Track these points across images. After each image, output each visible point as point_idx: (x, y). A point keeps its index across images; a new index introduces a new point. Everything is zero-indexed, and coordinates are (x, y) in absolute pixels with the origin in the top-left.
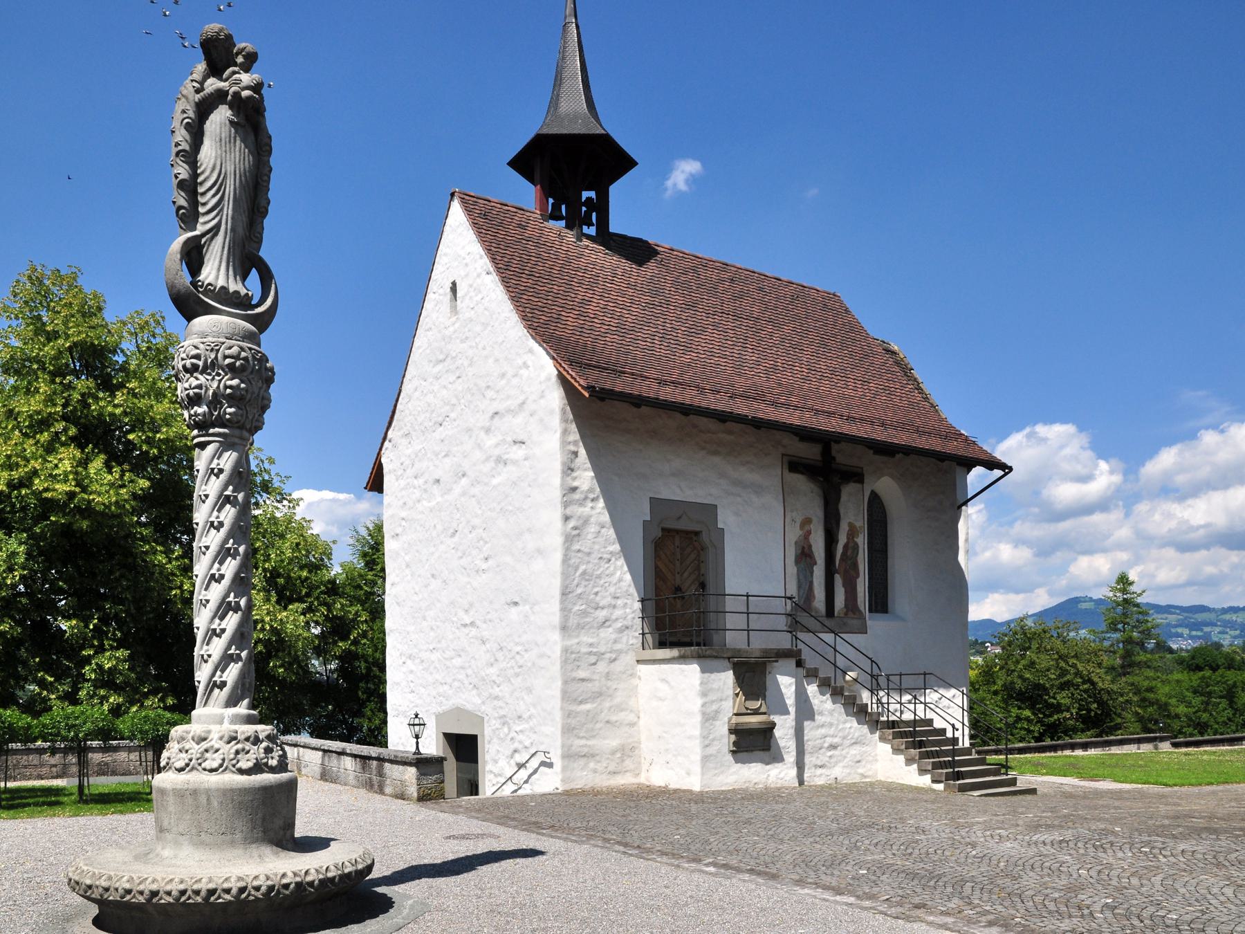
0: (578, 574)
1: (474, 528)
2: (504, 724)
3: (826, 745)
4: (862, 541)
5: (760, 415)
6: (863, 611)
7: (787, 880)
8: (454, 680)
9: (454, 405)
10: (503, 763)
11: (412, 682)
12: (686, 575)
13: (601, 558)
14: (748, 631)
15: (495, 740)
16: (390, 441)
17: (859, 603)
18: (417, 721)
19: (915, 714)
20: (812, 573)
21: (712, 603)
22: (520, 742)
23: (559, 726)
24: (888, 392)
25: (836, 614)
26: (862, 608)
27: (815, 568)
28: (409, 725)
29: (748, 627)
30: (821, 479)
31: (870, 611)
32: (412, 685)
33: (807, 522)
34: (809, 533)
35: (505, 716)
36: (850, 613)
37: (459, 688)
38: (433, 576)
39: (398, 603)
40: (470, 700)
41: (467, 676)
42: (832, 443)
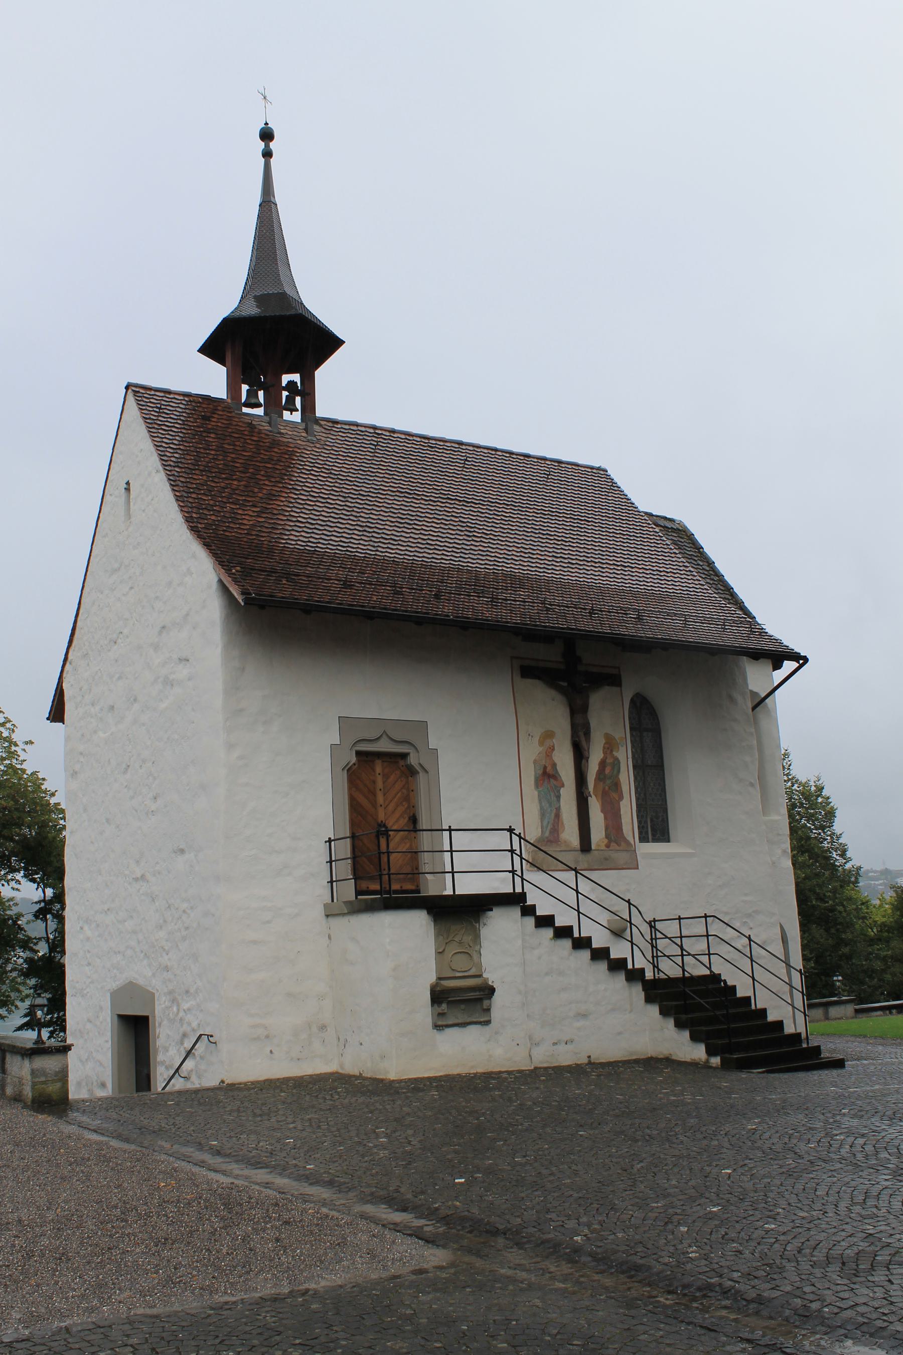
1: (144, 761)
4: (625, 756)
9: (127, 620)
10: (172, 1051)
11: (89, 952)
12: (391, 807)
15: (165, 1022)
16: (70, 663)
17: (624, 831)
19: (684, 970)
20: (558, 797)
25: (593, 847)
26: (630, 839)
27: (562, 791)
29: (453, 868)
30: (565, 684)
32: (88, 955)
33: (548, 735)
36: (612, 844)
38: (108, 820)
41: (139, 942)
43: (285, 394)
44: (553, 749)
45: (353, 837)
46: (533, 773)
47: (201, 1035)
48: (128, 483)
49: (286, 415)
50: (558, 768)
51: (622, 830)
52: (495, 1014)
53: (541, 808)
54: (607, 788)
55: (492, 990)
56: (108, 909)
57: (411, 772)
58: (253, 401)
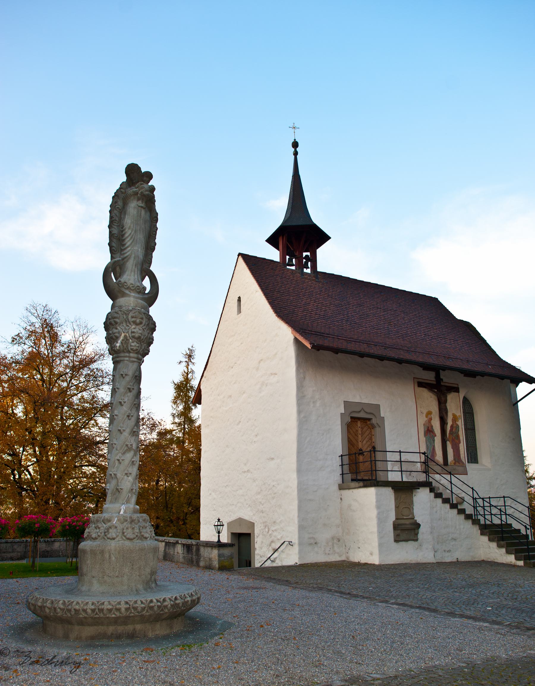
0: (306, 441)
2: (266, 527)
3: (450, 538)
4: (461, 423)
5: (401, 357)
6: (465, 462)
7: (443, 613)
8: (238, 502)
10: (265, 549)
12: (364, 442)
13: (318, 433)
14: (401, 471)
17: (461, 457)
18: (219, 524)
19: (501, 520)
20: (434, 441)
21: (379, 456)
22: (275, 536)
23: (297, 526)
24: (468, 345)
25: (449, 464)
26: (464, 461)
27: (435, 438)
28: (215, 526)
30: (436, 390)
31: (468, 462)
32: (214, 506)
33: (429, 413)
34: (431, 419)
35: (266, 522)
36: (457, 463)
37: (240, 507)
39: (207, 462)
40: (247, 515)
42: (441, 371)
43: (304, 260)
44: (432, 419)
45: (349, 455)
46: (423, 430)
47: (284, 542)
48: (239, 298)
49: (305, 270)
50: (434, 428)
51: (460, 457)
52: (420, 536)
53: (427, 446)
54: (454, 438)
55: (418, 526)
56: (227, 486)
57: (373, 427)
58: (291, 263)
